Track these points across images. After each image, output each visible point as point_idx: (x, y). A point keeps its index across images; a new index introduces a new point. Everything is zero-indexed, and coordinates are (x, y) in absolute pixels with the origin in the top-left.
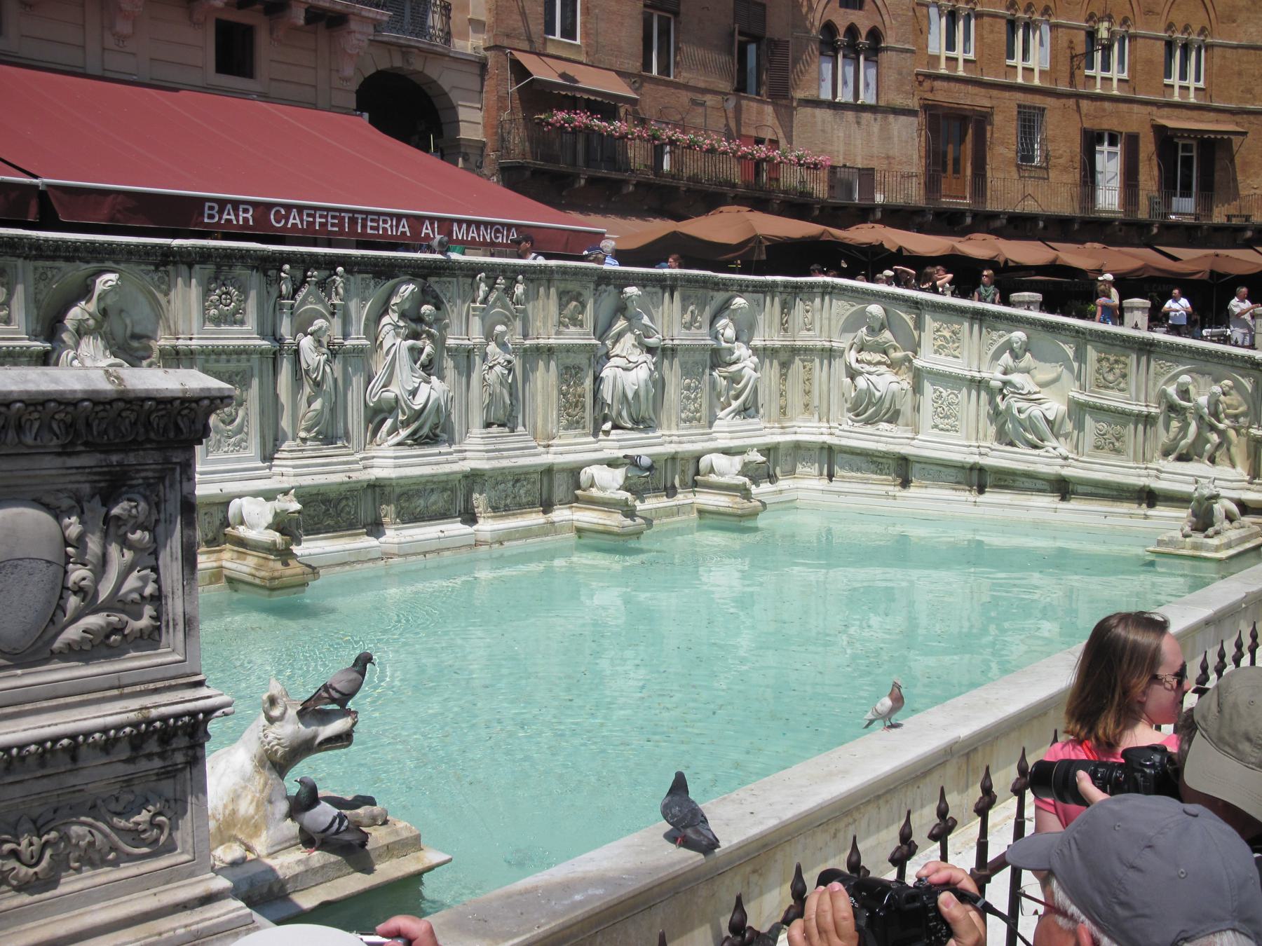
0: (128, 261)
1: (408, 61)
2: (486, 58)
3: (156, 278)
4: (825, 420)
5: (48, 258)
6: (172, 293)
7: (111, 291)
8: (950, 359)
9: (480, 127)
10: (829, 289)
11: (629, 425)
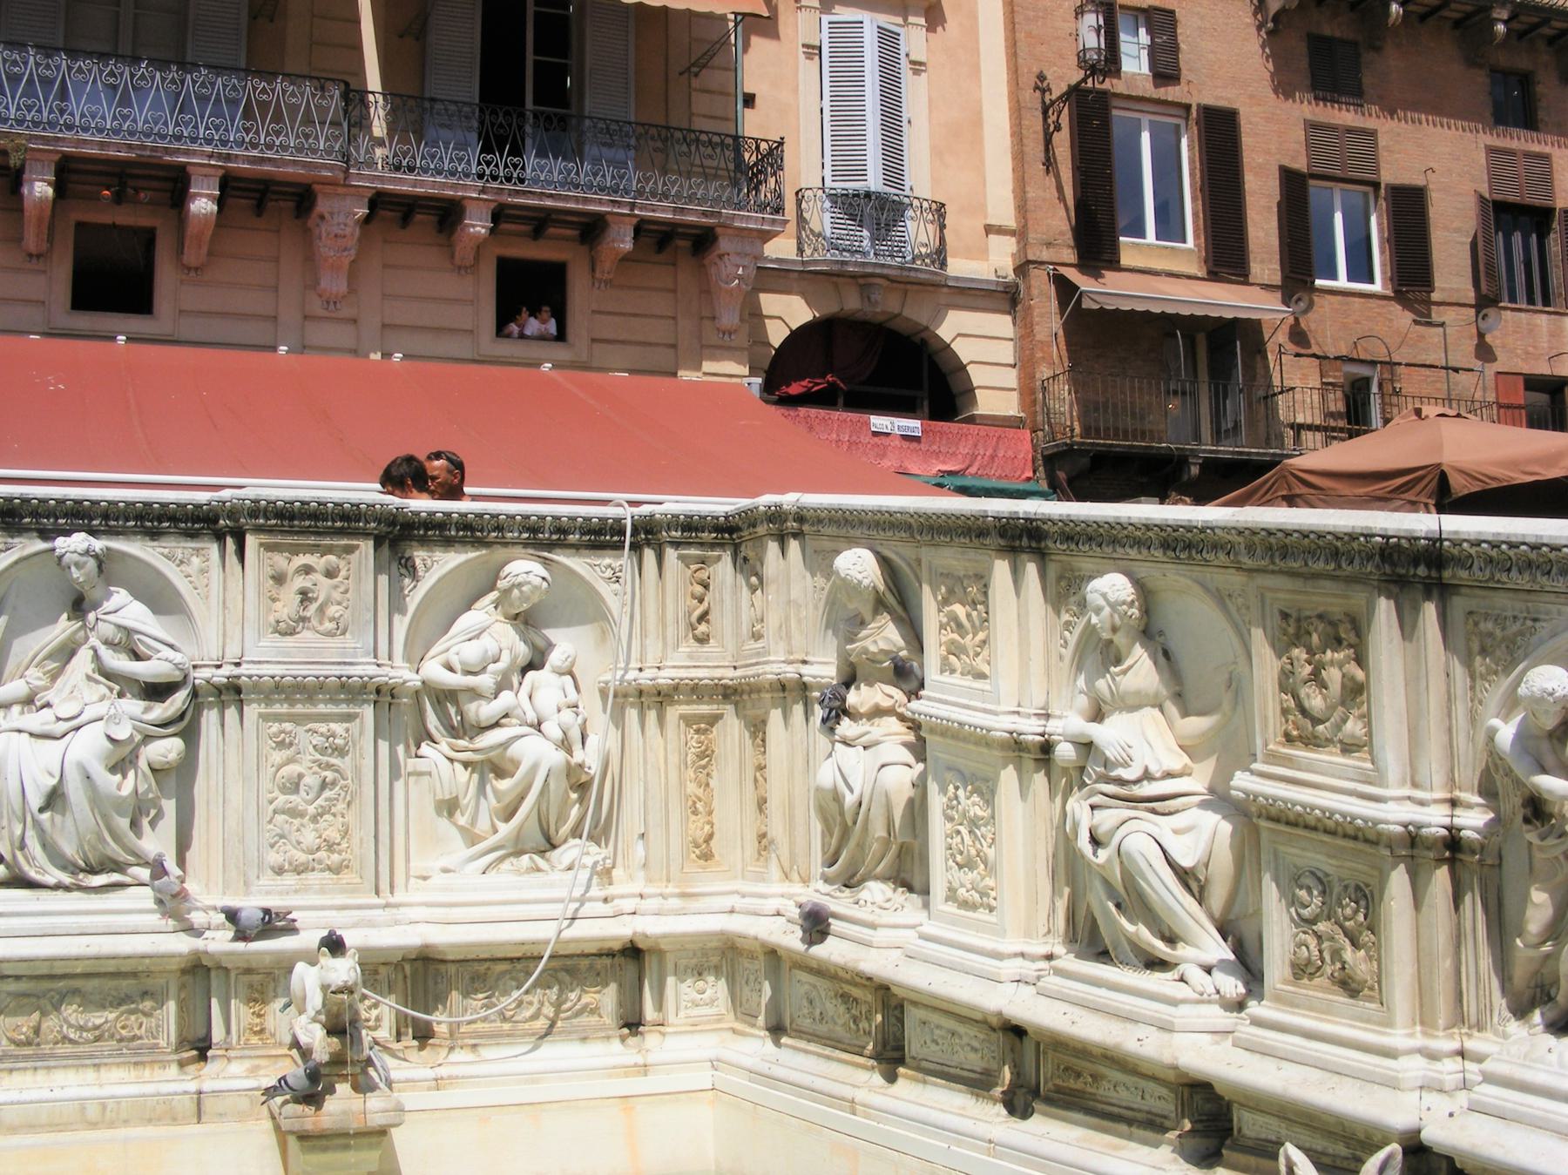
1: (869, 298)
2: (1017, 286)
4: (795, 876)
8: (968, 681)
9: (1015, 395)
10: (792, 525)
11: (54, 875)
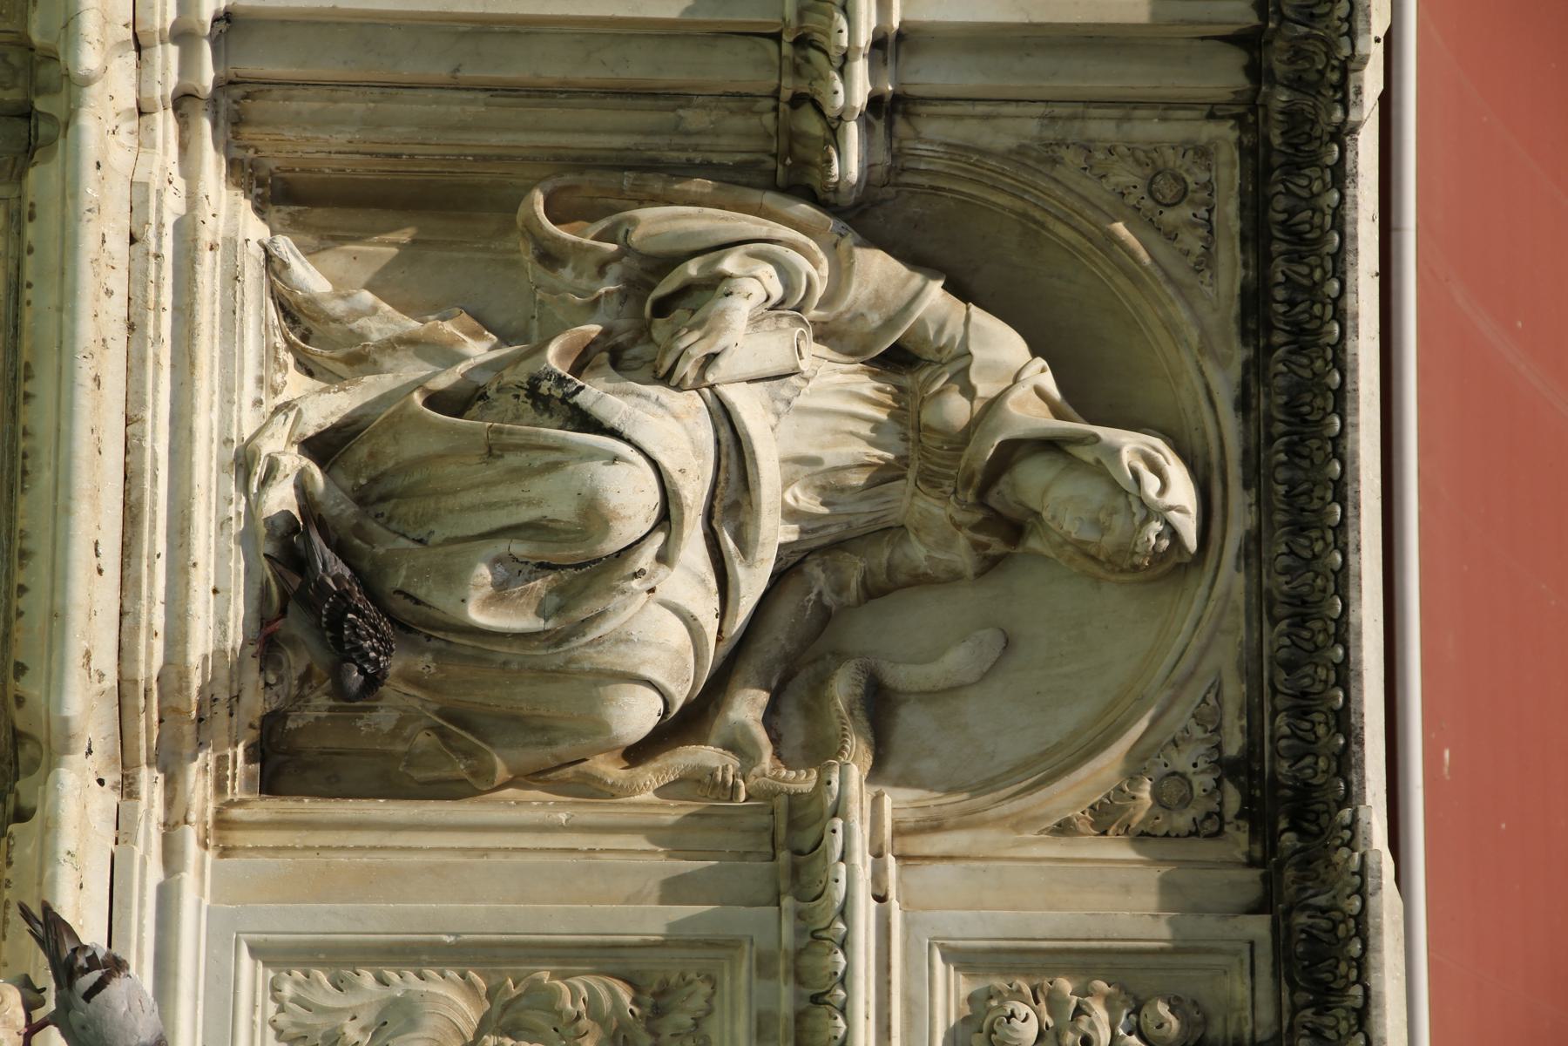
0: (1261, 604)
3: (1182, 761)
5: (1255, 206)
6: (1118, 850)
7: (1116, 487)
